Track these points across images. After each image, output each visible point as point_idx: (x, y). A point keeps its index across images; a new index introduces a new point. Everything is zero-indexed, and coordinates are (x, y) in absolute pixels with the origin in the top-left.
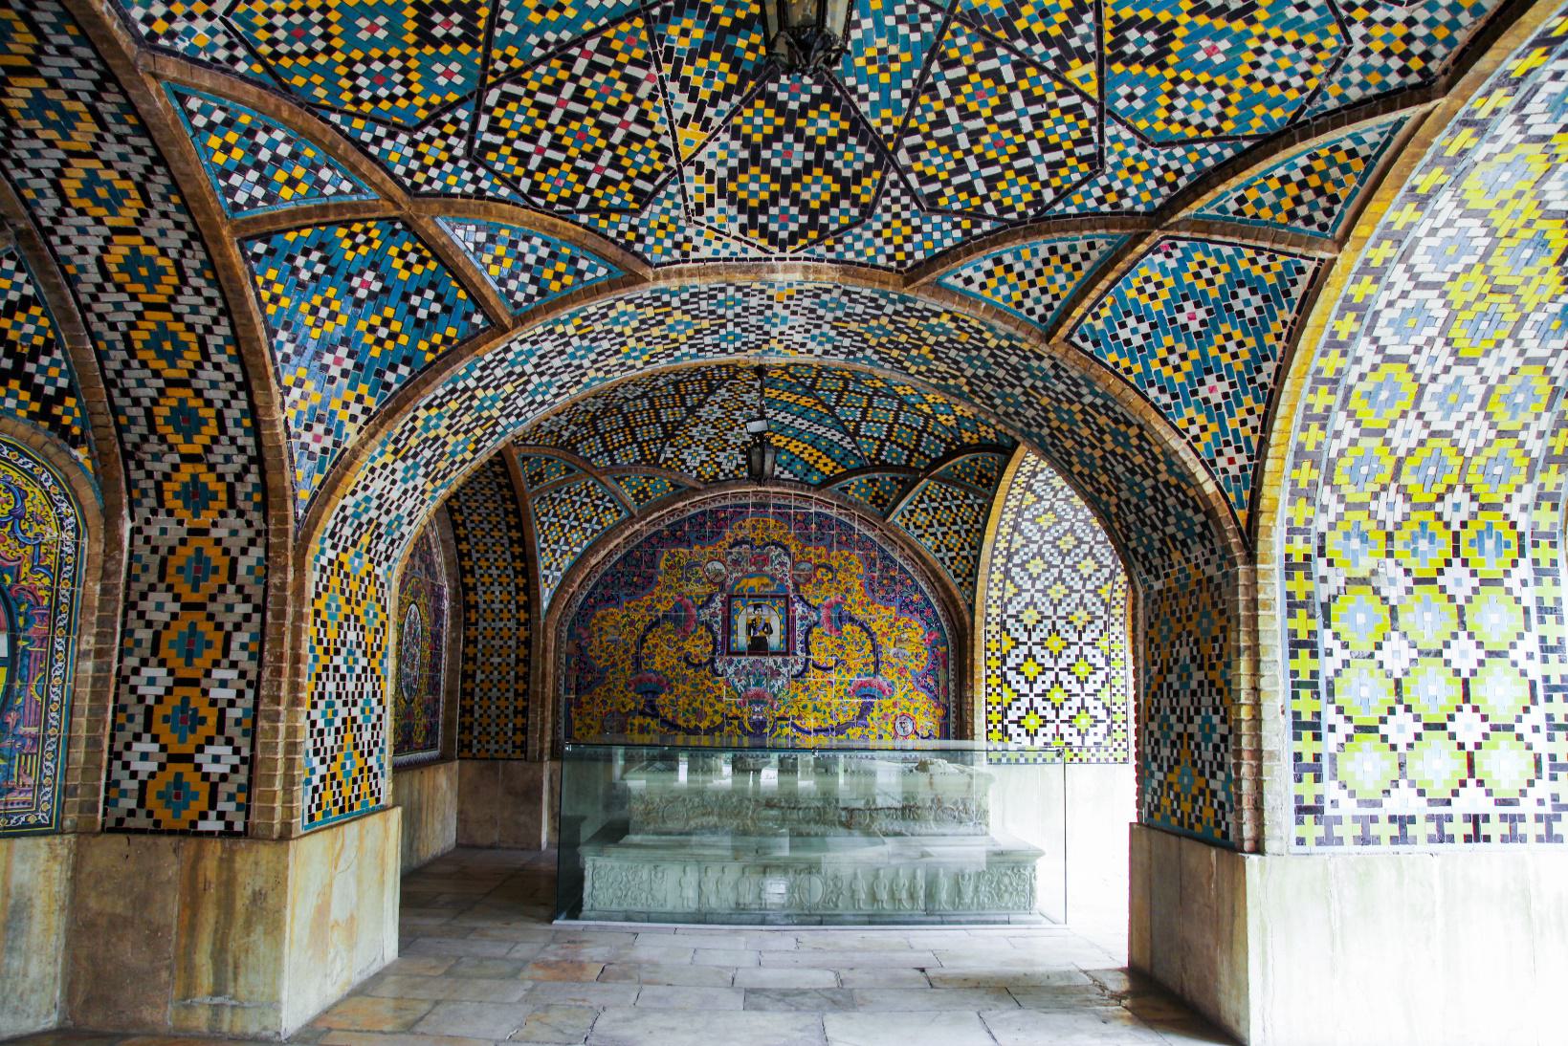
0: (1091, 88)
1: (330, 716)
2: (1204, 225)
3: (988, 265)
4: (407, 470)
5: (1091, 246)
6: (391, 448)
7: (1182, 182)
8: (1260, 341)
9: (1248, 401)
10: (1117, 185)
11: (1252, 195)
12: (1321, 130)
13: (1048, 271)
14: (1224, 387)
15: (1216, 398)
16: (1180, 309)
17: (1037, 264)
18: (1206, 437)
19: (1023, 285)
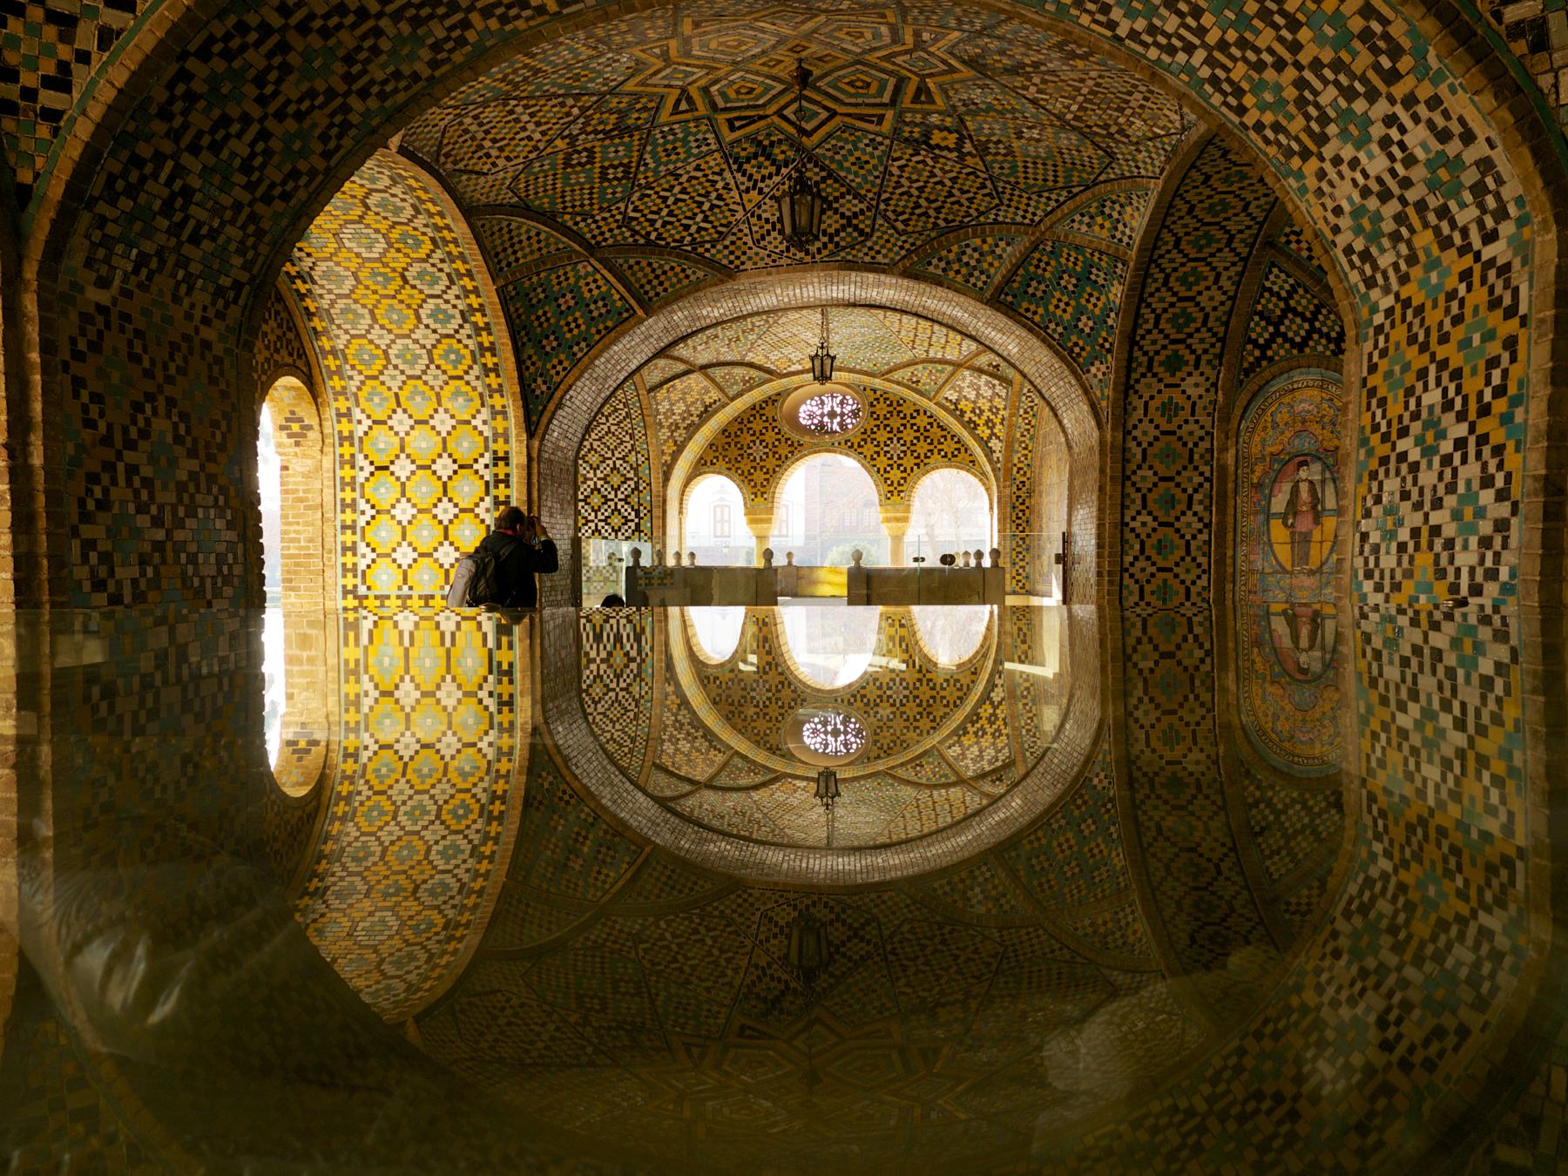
1: (1390, 526)
4: (1344, 134)
6: (1296, 162)
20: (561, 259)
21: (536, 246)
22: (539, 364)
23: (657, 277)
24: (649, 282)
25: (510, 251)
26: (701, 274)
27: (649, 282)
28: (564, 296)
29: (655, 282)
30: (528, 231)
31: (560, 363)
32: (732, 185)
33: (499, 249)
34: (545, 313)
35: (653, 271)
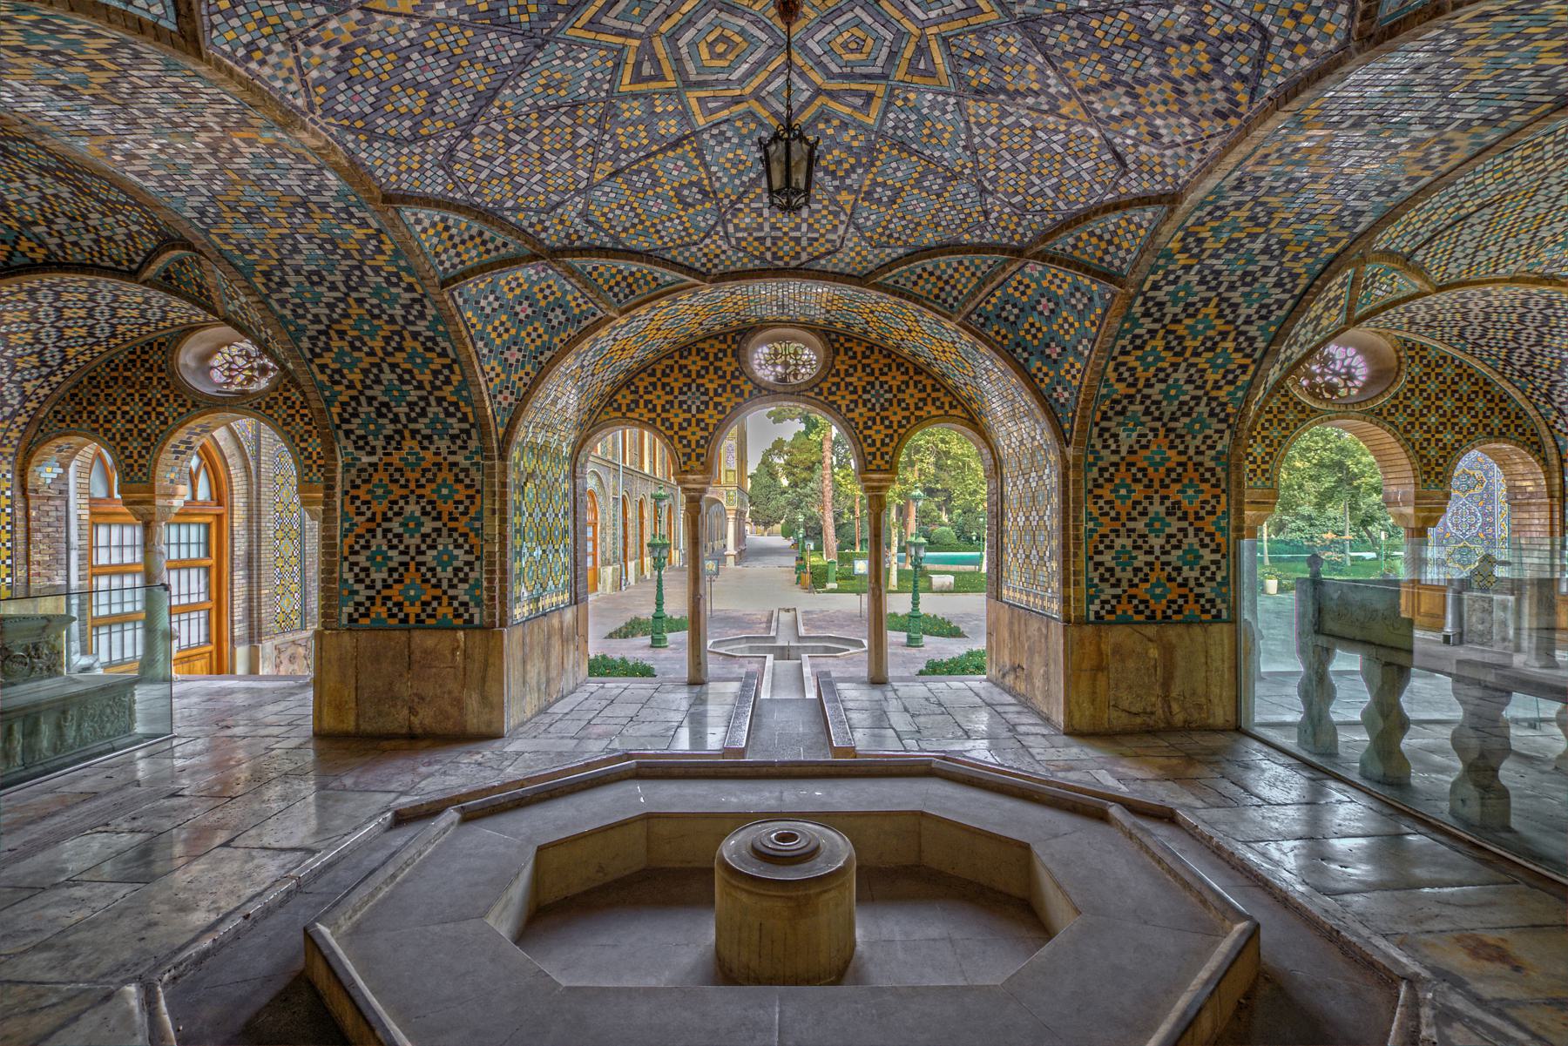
0: (598, 176)
2: (572, 272)
3: (437, 218)
5: (505, 245)
7: (577, 243)
8: (551, 338)
9: (528, 368)
10: (548, 224)
11: (601, 269)
12: (656, 264)
13: (470, 244)
14: (519, 356)
15: (512, 360)
16: (520, 303)
17: (466, 236)
18: (497, 381)
19: (449, 244)
20: (997, 274)
21: (968, 274)
22: (1051, 373)
23: (1110, 242)
24: (1106, 252)
25: (948, 288)
26: (1149, 215)
27: (1106, 252)
28: (1039, 302)
29: (1112, 249)
30: (949, 265)
31: (1072, 366)
32: (1035, 115)
33: (936, 291)
34: (1032, 325)
35: (1100, 238)
